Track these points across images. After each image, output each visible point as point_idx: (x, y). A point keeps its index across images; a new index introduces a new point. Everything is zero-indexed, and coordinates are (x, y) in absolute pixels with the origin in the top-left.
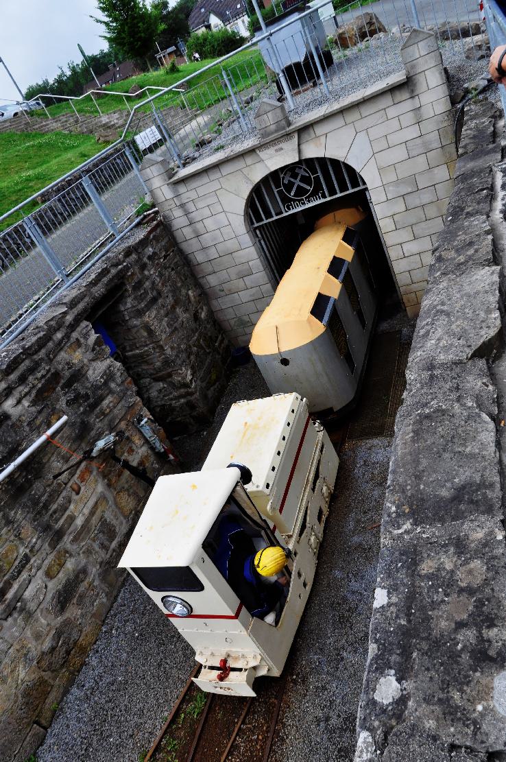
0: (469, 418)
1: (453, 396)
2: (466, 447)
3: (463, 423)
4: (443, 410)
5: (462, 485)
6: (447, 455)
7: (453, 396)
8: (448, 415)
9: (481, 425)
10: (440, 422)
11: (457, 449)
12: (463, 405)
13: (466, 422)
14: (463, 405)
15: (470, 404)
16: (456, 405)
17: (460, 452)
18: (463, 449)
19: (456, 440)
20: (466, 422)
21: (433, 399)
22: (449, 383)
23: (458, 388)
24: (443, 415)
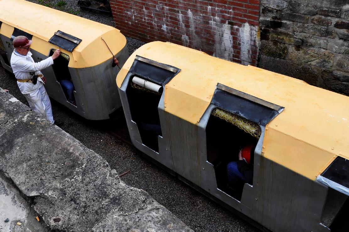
0: (42, 183)
1: (70, 192)
2: (27, 166)
3: (43, 178)
4: (66, 177)
5: (13, 148)
6: (35, 155)
7: (70, 192)
8: (58, 176)
9: (30, 184)
10: (60, 169)
11: (32, 161)
12: (55, 189)
13: (41, 179)
14: (55, 189)
15: (50, 193)
16: (59, 186)
17: (29, 161)
18: (29, 164)
19: (37, 165)
20: (41, 179)
21: (83, 180)
22: (84, 200)
23: (73, 200)
24: (62, 174)
